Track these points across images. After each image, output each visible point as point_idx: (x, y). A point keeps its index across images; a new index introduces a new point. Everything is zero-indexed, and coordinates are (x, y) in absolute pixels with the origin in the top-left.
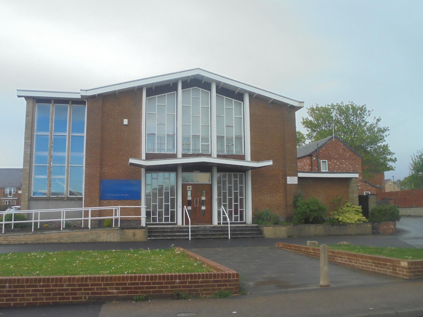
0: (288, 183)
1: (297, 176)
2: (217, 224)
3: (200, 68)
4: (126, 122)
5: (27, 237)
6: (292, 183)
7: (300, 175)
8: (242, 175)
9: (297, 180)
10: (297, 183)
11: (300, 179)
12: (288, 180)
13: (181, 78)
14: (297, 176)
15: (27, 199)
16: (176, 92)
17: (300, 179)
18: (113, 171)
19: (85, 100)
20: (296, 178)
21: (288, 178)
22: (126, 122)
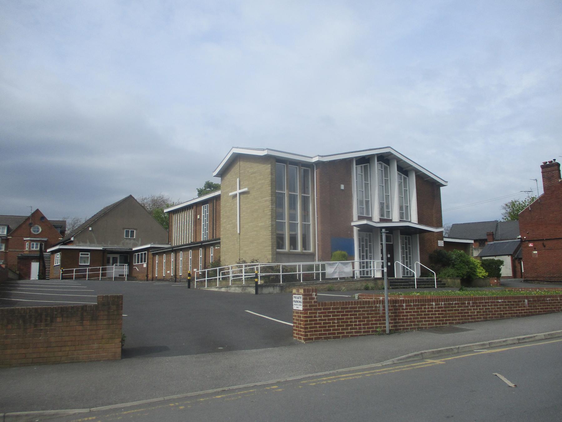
0: (439, 245)
1: (443, 240)
2: (402, 277)
3: (391, 147)
4: (342, 187)
5: (319, 286)
8: (409, 238)
9: (443, 244)
10: (443, 246)
11: (445, 242)
12: (439, 243)
13: (377, 154)
14: (443, 240)
15: (275, 252)
16: (369, 164)
17: (445, 242)
19: (314, 165)
20: (443, 242)
21: (439, 241)
22: (342, 187)
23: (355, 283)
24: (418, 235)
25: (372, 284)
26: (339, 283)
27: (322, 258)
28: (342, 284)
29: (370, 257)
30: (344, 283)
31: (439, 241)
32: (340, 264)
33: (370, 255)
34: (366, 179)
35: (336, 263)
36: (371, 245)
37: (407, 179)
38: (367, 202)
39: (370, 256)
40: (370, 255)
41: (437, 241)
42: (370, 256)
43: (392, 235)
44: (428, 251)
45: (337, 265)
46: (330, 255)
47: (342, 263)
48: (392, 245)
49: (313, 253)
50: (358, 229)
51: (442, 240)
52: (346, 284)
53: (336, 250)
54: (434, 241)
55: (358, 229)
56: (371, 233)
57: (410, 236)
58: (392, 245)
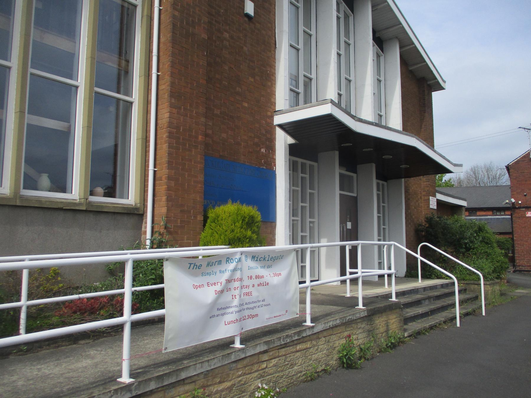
1: (436, 197)
6: (433, 207)
7: (440, 197)
11: (439, 202)
17: (439, 202)
18: (224, 135)
21: (431, 197)
23: (308, 345)
24: (403, 180)
25: (360, 336)
26: (240, 365)
27: (166, 228)
28: (256, 367)
29: (310, 228)
30: (265, 357)
31: (431, 197)
32: (250, 263)
33: (310, 222)
34: (307, 23)
35: (228, 259)
36: (313, 194)
37: (382, 59)
38: (308, 81)
39: (311, 225)
40: (310, 222)
41: (426, 198)
42: (311, 225)
43: (354, 175)
44: (414, 217)
45: (232, 266)
46: (200, 218)
47: (254, 257)
48: (355, 200)
49: (137, 209)
50: (291, 140)
51: (434, 196)
52: (274, 362)
53: (224, 202)
54: (421, 198)
55: (291, 140)
56: (315, 164)
57: (385, 183)
58: (355, 199)
